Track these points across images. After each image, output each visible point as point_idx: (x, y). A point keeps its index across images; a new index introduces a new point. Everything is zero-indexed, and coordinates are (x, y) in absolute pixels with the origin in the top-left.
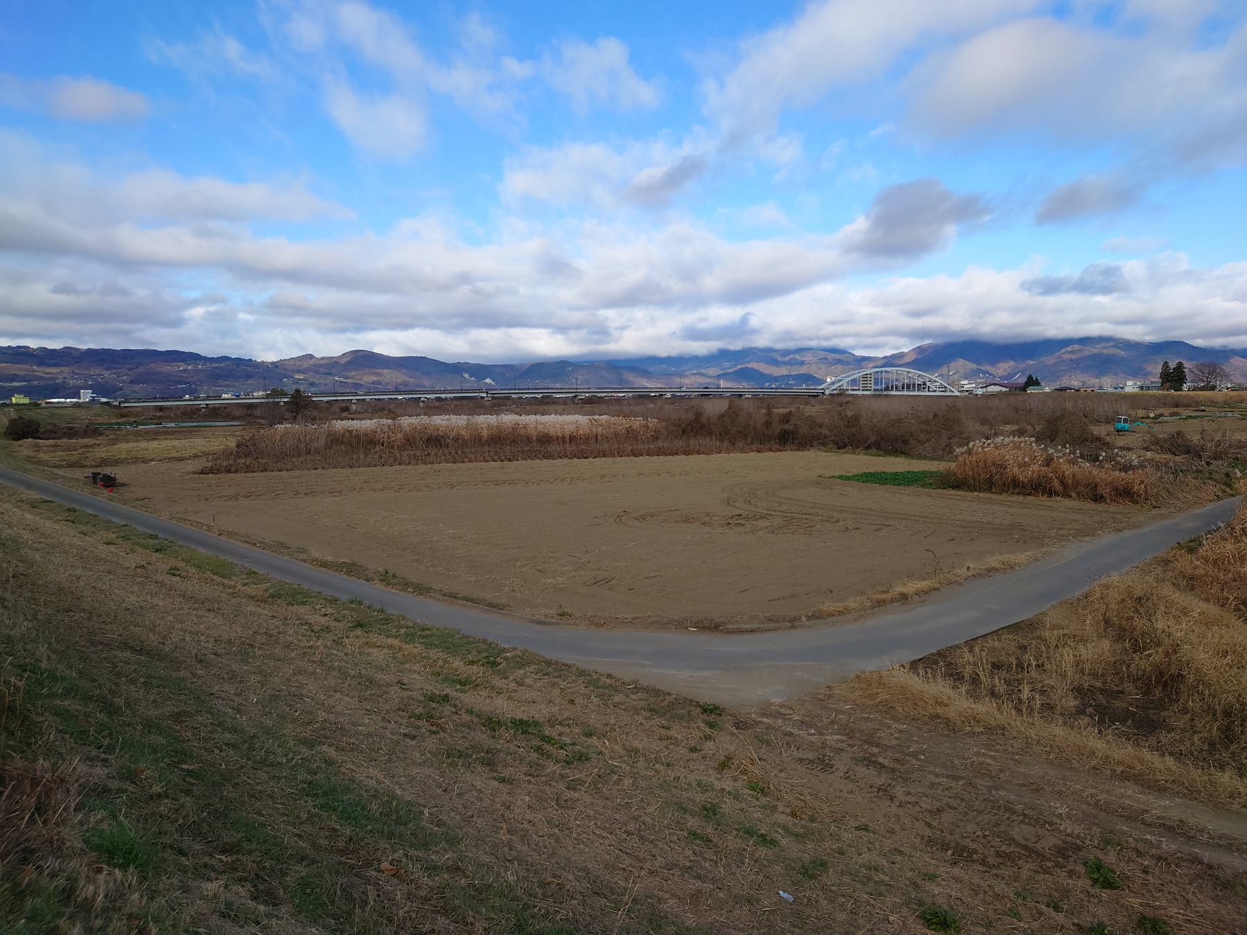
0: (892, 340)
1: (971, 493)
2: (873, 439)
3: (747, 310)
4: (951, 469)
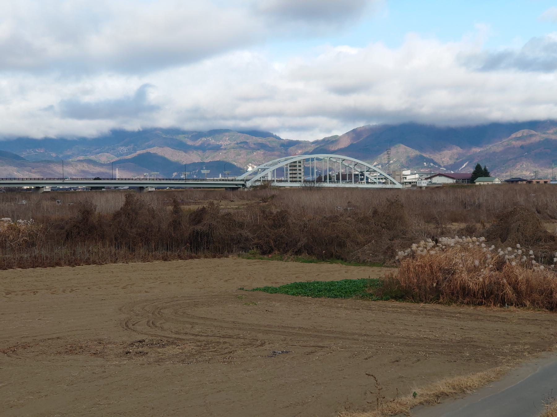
0: (322, 120)
1: (416, 305)
2: (304, 241)
3: (146, 80)
4: (394, 277)
